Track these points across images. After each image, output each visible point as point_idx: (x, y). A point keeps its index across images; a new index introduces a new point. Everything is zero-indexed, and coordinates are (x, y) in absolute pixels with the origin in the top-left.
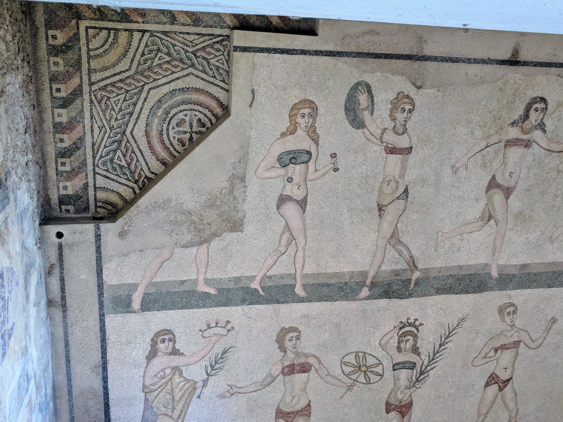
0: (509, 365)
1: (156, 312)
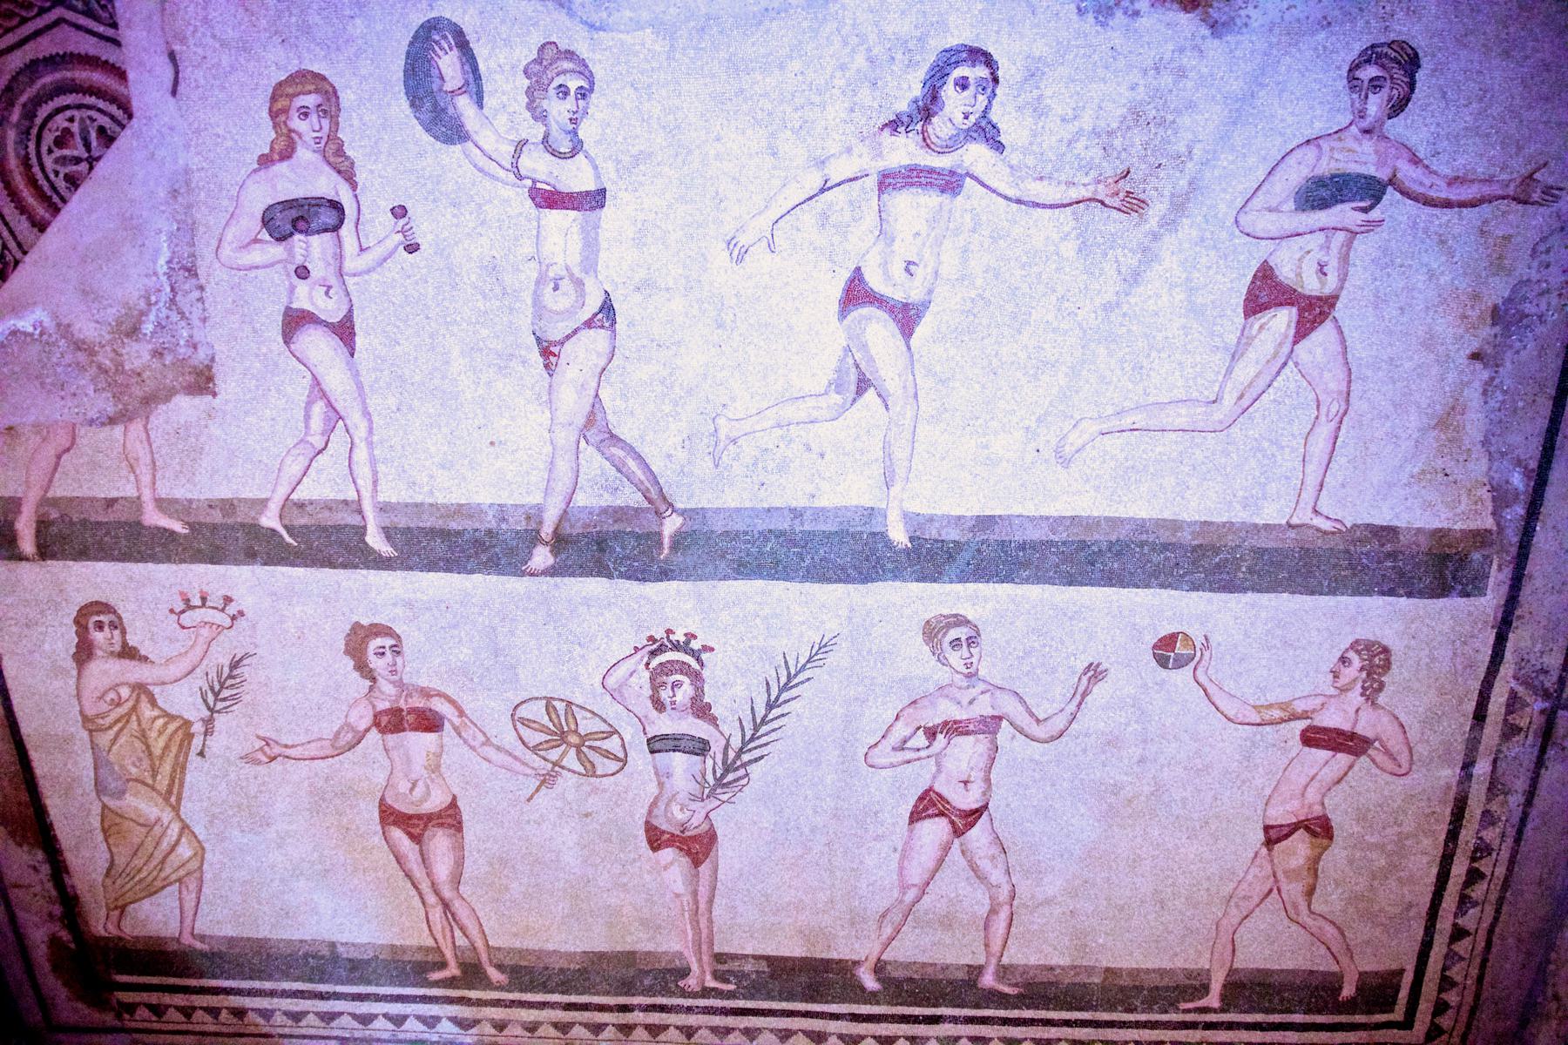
0: (973, 774)
1: (71, 563)
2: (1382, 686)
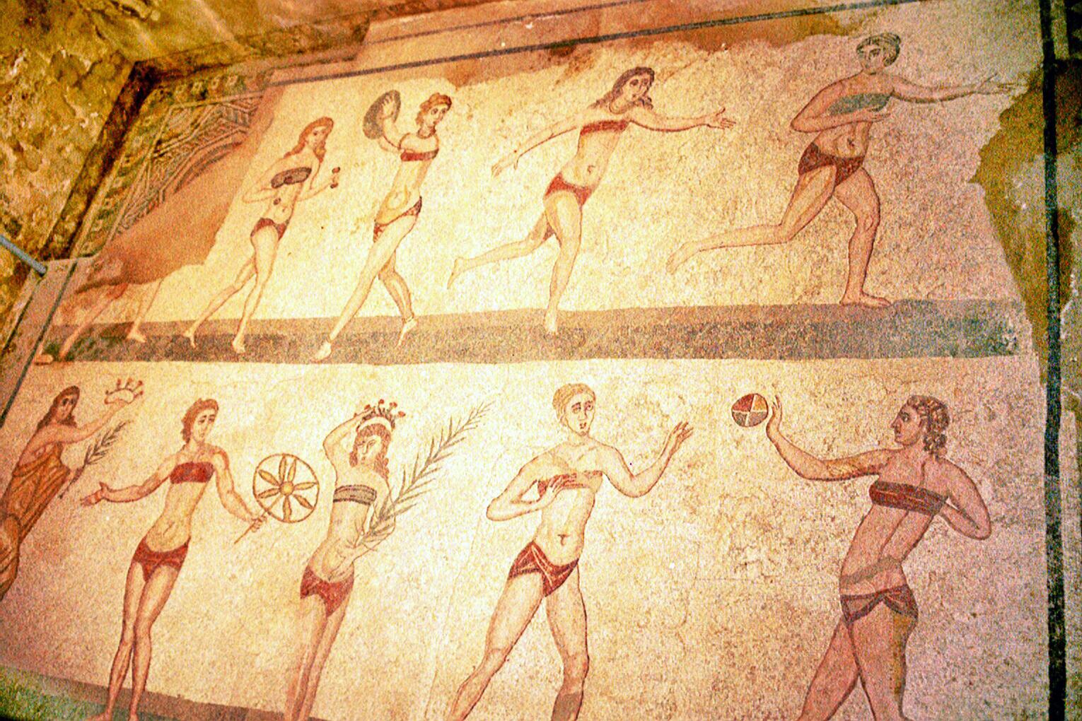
2: (942, 442)
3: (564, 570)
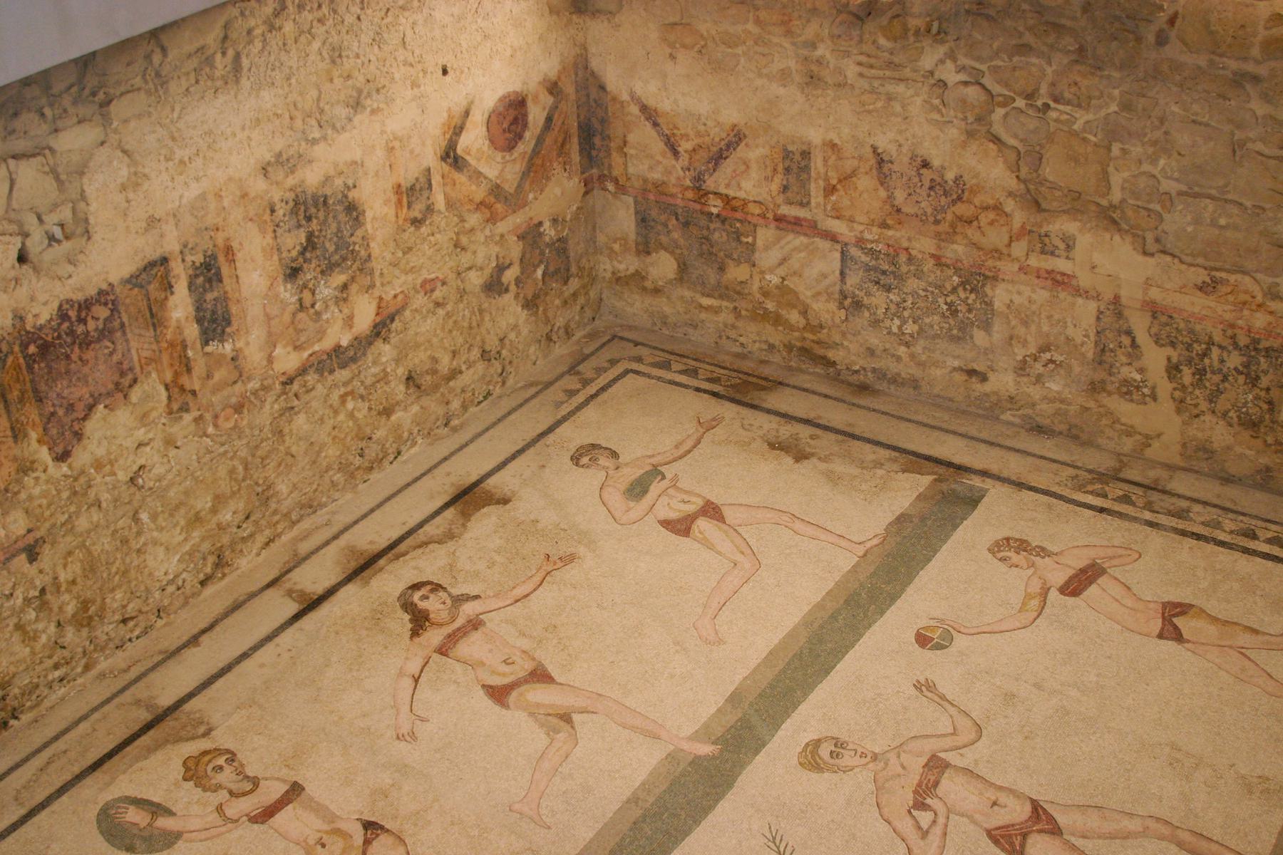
2: (1043, 549)
3: (1038, 813)
